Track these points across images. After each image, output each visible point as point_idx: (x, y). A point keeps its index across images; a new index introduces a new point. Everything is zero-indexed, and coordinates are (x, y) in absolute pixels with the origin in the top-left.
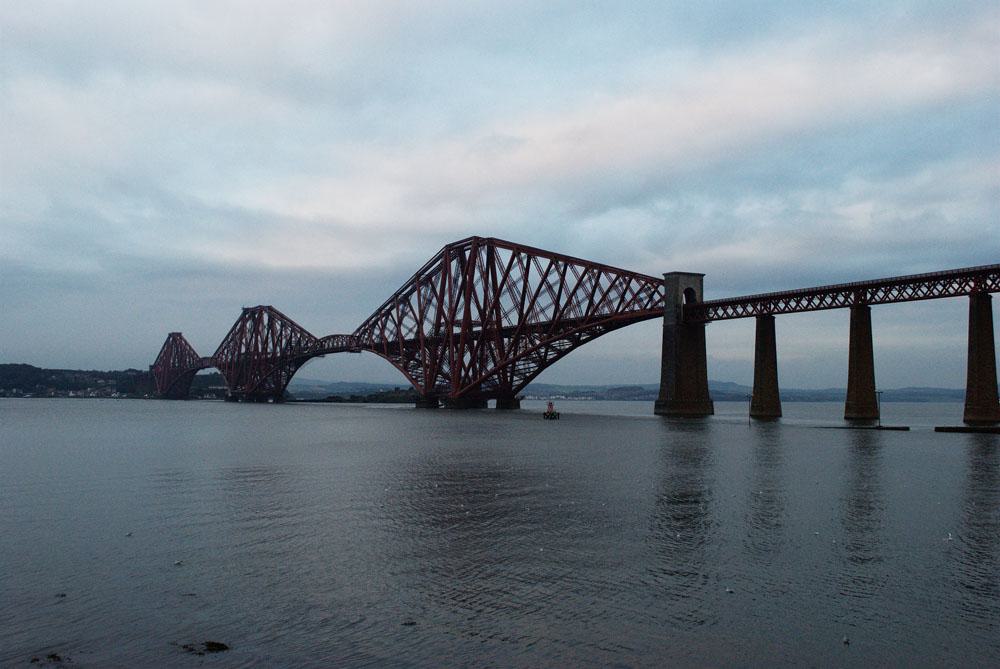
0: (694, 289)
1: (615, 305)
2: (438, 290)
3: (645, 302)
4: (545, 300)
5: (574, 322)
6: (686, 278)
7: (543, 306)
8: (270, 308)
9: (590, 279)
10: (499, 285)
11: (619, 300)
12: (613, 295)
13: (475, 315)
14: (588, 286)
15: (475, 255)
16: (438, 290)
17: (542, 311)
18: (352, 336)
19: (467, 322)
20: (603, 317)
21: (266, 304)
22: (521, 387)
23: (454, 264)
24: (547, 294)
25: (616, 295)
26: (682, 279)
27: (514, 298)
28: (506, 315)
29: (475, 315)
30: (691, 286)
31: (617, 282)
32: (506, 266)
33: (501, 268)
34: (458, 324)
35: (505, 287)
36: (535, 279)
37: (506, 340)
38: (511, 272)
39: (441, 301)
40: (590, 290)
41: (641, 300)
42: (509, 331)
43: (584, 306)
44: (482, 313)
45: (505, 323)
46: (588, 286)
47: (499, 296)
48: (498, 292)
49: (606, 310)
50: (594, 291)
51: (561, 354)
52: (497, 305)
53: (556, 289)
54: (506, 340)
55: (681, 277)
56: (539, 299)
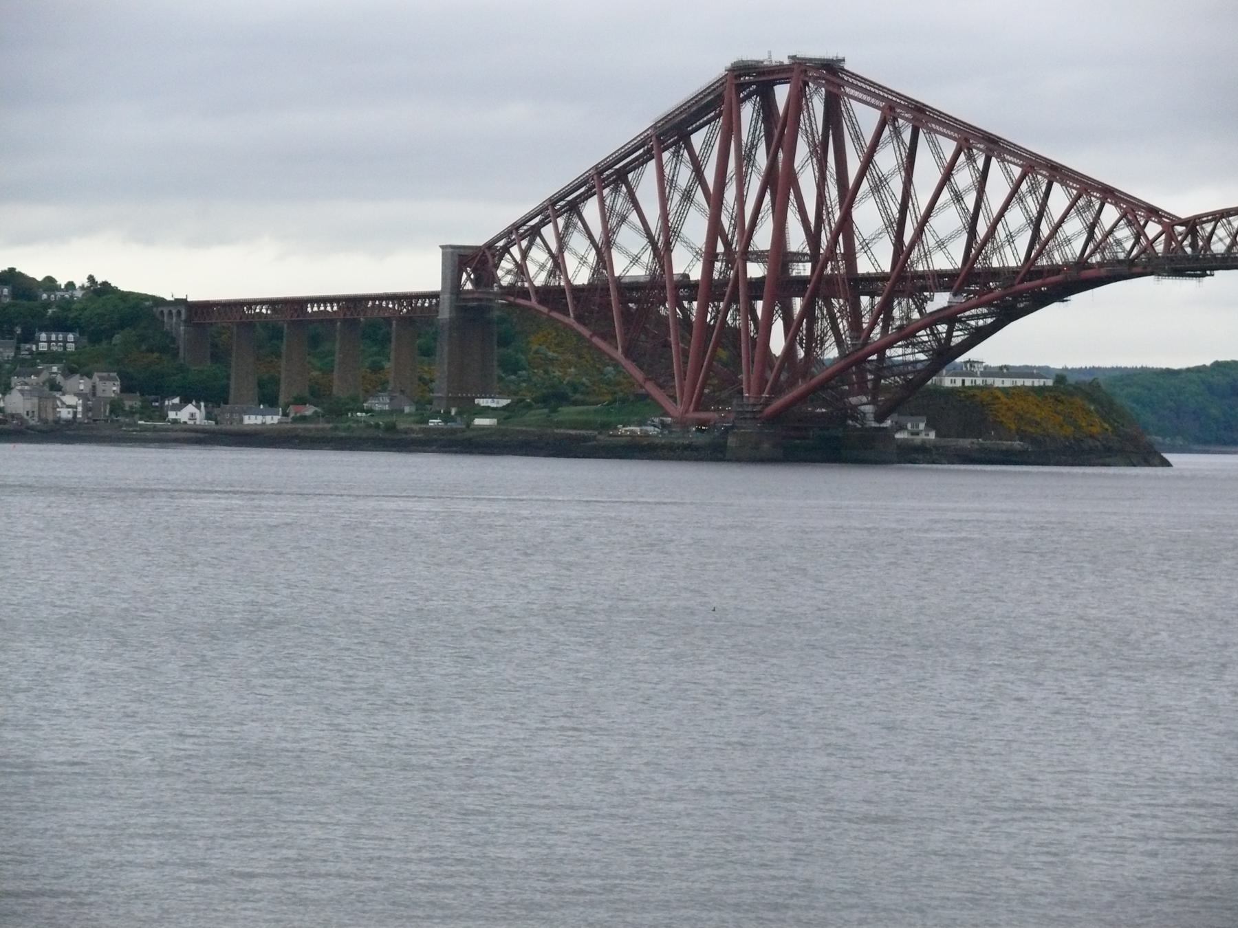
1: (1078, 245)
2: (710, 174)
3: (1128, 245)
4: (948, 221)
9: (1033, 190)
10: (851, 184)
11: (1085, 236)
12: (1074, 226)
13: (797, 240)
15: (798, 101)
16: (710, 174)
17: (941, 245)
19: (780, 256)
20: (1054, 270)
23: (748, 112)
27: (884, 209)
28: (866, 245)
29: (797, 240)
32: (868, 138)
33: (857, 137)
34: (759, 257)
35: (865, 185)
36: (927, 172)
37: (865, 300)
38: (877, 158)
39: (716, 202)
40: (1035, 212)
41: (1118, 242)
42: (870, 283)
43: (1023, 242)
44: (813, 238)
45: (864, 266)
46: (1032, 205)
47: (850, 207)
48: (848, 198)
49: (1058, 258)
50: (1041, 214)
52: (846, 225)
53: (970, 201)
54: (865, 300)
56: (932, 221)
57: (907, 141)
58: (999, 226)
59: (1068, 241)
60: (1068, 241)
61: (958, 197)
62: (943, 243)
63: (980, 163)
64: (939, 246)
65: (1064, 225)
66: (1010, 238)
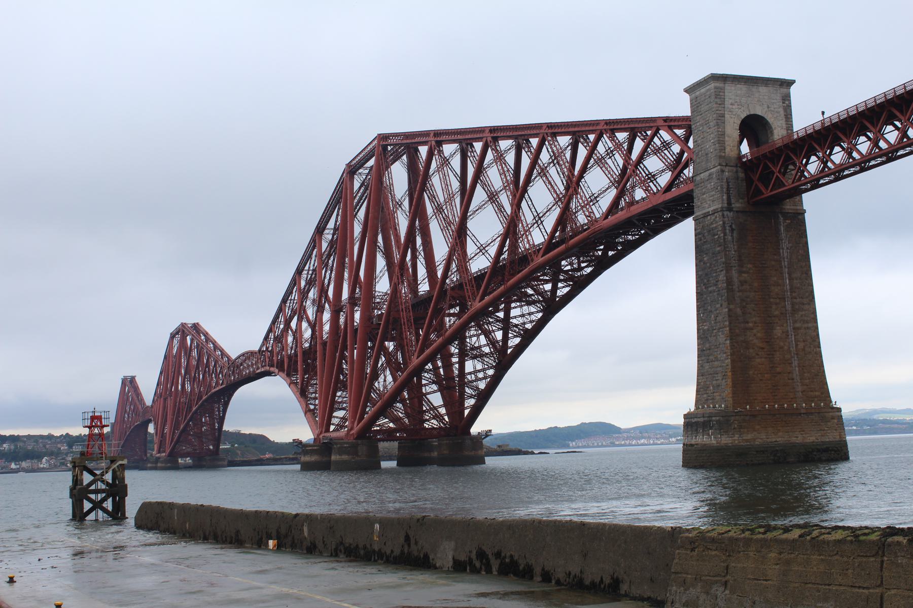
0: (769, 118)
5: (525, 259)
6: (742, 88)
7: (483, 241)
8: (196, 327)
9: (556, 158)
14: (553, 171)
18: (260, 350)
21: (190, 321)
22: (477, 410)
24: (490, 209)
25: (604, 182)
26: (732, 92)
30: (759, 111)
31: (601, 148)
40: (562, 188)
41: (652, 177)
51: (528, 337)
55: (731, 92)
57: (458, 170)
58: (524, 204)
59: (594, 199)
60: (594, 199)
61: (493, 197)
62: (484, 248)
63: (510, 158)
64: (481, 251)
65: (588, 177)
66: (539, 219)
